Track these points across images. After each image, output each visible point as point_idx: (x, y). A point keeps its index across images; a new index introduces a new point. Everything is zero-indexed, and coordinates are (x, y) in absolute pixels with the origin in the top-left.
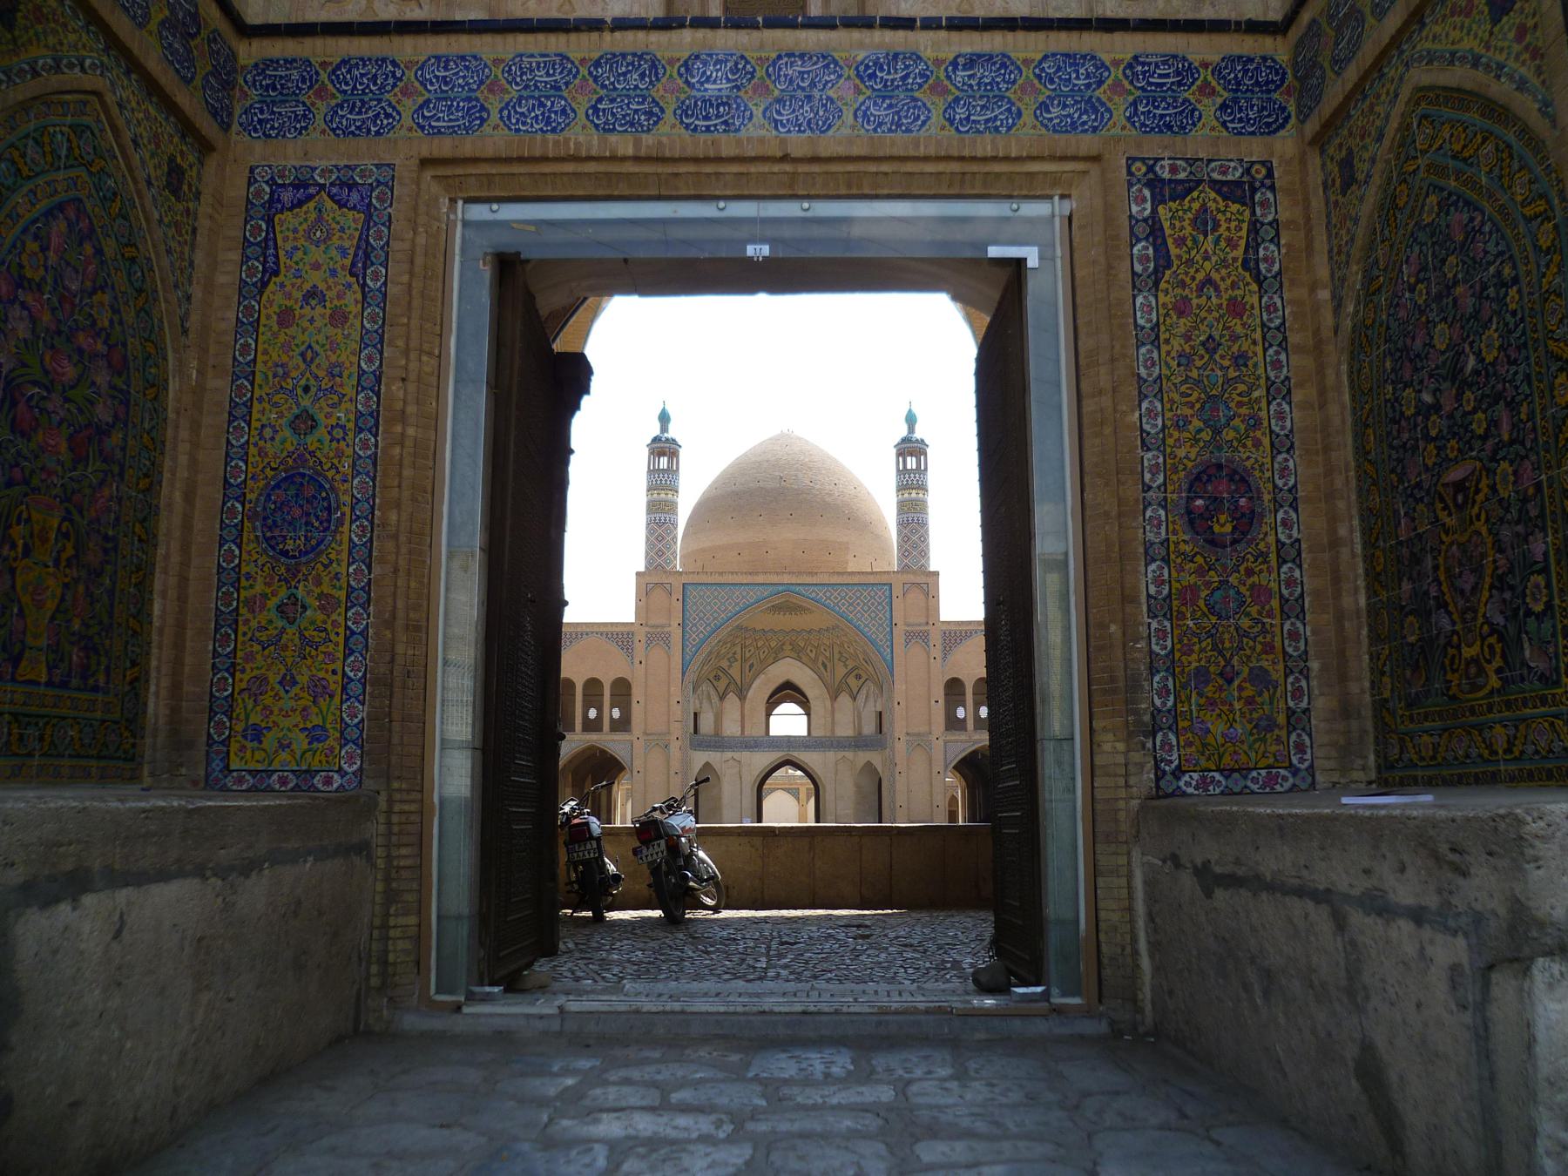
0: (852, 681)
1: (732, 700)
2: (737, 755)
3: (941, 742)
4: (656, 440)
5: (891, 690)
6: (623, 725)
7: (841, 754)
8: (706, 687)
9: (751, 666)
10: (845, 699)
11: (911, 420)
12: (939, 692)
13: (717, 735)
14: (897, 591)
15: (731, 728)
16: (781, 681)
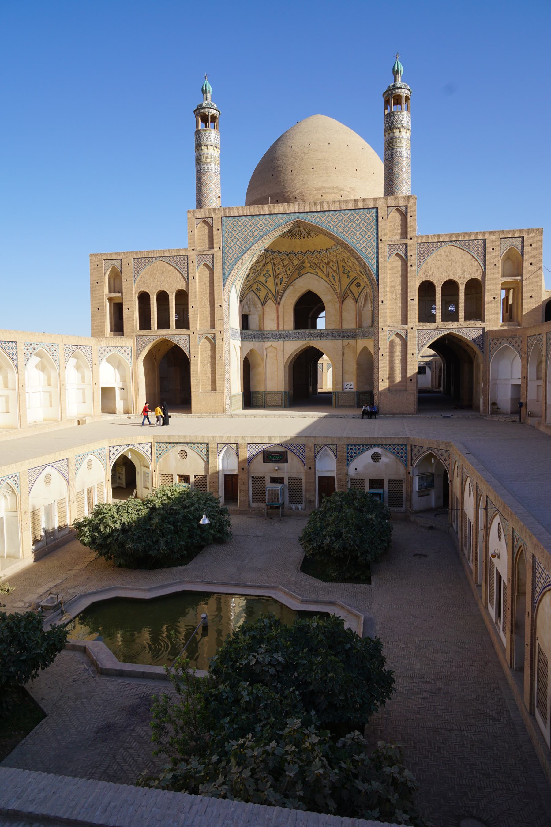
0: (354, 288)
1: (270, 304)
4: (200, 107)
6: (183, 322)
7: (346, 342)
8: (251, 295)
9: (282, 280)
10: (349, 303)
12: (414, 293)
15: (270, 325)
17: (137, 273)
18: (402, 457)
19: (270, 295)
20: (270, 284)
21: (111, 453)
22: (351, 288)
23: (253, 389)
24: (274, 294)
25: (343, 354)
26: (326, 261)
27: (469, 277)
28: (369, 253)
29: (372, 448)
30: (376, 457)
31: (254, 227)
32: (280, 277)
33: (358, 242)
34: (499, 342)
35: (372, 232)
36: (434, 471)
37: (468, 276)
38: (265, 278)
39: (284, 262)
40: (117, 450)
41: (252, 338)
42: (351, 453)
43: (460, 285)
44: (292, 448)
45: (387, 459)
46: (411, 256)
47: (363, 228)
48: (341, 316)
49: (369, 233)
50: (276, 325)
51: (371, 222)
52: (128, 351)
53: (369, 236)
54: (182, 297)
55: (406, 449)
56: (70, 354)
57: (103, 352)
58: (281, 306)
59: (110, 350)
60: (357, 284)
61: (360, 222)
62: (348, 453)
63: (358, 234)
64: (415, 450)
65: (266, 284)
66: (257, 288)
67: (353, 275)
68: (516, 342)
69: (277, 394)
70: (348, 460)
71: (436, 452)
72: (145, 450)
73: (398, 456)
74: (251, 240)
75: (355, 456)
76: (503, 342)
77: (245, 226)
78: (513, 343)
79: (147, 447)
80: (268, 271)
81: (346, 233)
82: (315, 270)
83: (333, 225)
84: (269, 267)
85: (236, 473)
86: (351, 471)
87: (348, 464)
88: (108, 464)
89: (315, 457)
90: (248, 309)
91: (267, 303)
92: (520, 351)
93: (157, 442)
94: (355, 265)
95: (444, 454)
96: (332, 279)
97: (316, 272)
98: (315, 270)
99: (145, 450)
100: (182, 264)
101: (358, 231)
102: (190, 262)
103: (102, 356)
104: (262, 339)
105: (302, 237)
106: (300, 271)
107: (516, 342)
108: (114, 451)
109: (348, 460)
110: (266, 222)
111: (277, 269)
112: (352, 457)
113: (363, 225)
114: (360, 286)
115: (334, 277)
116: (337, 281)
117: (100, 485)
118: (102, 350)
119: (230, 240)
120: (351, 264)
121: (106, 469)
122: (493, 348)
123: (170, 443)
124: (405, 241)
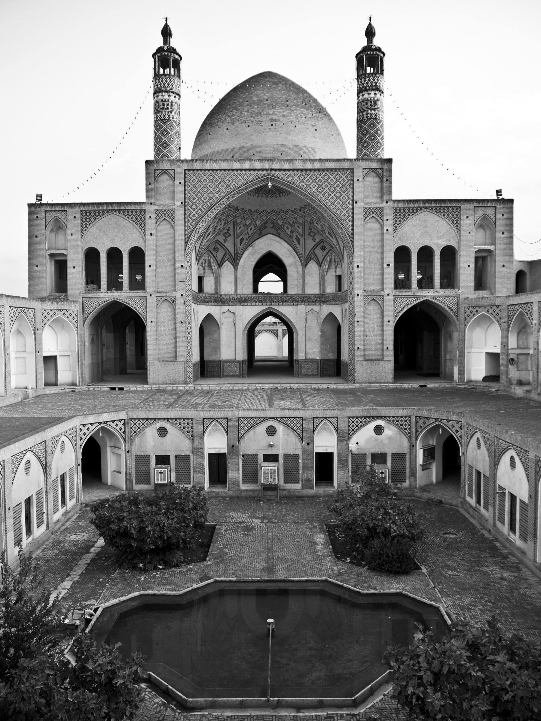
0: (319, 252)
1: (227, 265)
2: (232, 308)
3: (391, 296)
4: (160, 50)
5: (351, 255)
6: (138, 285)
7: (309, 307)
9: (242, 240)
10: (313, 266)
11: (370, 33)
12: (390, 258)
13: (216, 293)
14: (358, 174)
15: (227, 288)
16: (264, 251)
17: (84, 228)
18: (405, 429)
20: (229, 244)
21: (82, 432)
22: (315, 251)
23: (206, 358)
25: (306, 320)
26: (291, 222)
27: (444, 243)
28: (344, 216)
29: (375, 420)
30: (378, 430)
31: (220, 183)
32: (241, 237)
33: (333, 203)
34: (475, 310)
35: (347, 193)
36: (435, 444)
37: (444, 243)
38: (224, 238)
39: (247, 221)
40: (88, 429)
41: (208, 302)
42: (353, 426)
43: (436, 252)
44: (289, 422)
45: (390, 431)
46: (387, 220)
47: (338, 189)
48: (304, 281)
49: (344, 195)
50: (234, 289)
51: (346, 183)
52: (73, 315)
53: (344, 198)
54: (137, 255)
55: (410, 421)
56: (15, 318)
57: (47, 315)
59: (55, 314)
60: (322, 247)
61: (335, 183)
62: (349, 426)
63: (332, 195)
64: (421, 422)
65: (226, 244)
66: (214, 248)
67: (318, 238)
68: (494, 311)
69: (235, 362)
70: (349, 434)
71: (446, 423)
72: (118, 428)
73: (402, 428)
74: (217, 196)
75: (357, 430)
76: (479, 310)
77: (211, 181)
78: (491, 311)
79: (121, 425)
80: (228, 230)
81: (320, 193)
82: (277, 230)
83: (306, 185)
84: (231, 226)
85: (222, 451)
86: (352, 445)
87: (349, 438)
88: (78, 445)
89: (314, 431)
90: (202, 271)
91: (225, 264)
92: (499, 320)
93: (131, 419)
94: (324, 227)
95: (455, 425)
96: (295, 241)
97: (278, 233)
98: (277, 230)
99: (118, 428)
100: (138, 219)
101: (332, 192)
102: (147, 217)
103: (46, 320)
105: (269, 196)
106: (261, 233)
107: (494, 311)
108: (85, 430)
109: (349, 434)
110: (234, 178)
111: (238, 228)
112: (353, 430)
113: (338, 186)
114: (325, 250)
115: (298, 240)
116: (301, 243)
117: (71, 470)
118: (45, 314)
119: (194, 195)
120: (319, 227)
121: (76, 452)
122: (468, 316)
123: (147, 419)
124: (380, 205)
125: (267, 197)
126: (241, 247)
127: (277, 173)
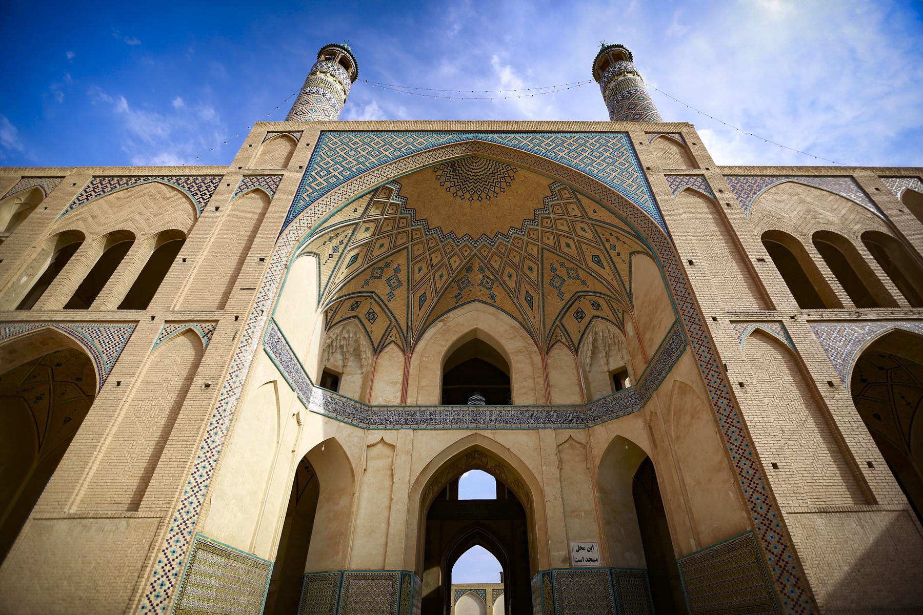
0: (570, 323)
9: (423, 299)
10: (561, 354)
15: (386, 393)
19: (394, 331)
20: (398, 306)
24: (404, 329)
38: (388, 290)
48: (547, 378)
58: (415, 356)
60: (577, 312)
65: (390, 305)
66: (369, 313)
80: (397, 270)
96: (525, 304)
104: (362, 421)
105: (476, 196)
114: (582, 318)
115: (529, 299)
125: (471, 199)
126: (421, 315)
127: (490, 136)
